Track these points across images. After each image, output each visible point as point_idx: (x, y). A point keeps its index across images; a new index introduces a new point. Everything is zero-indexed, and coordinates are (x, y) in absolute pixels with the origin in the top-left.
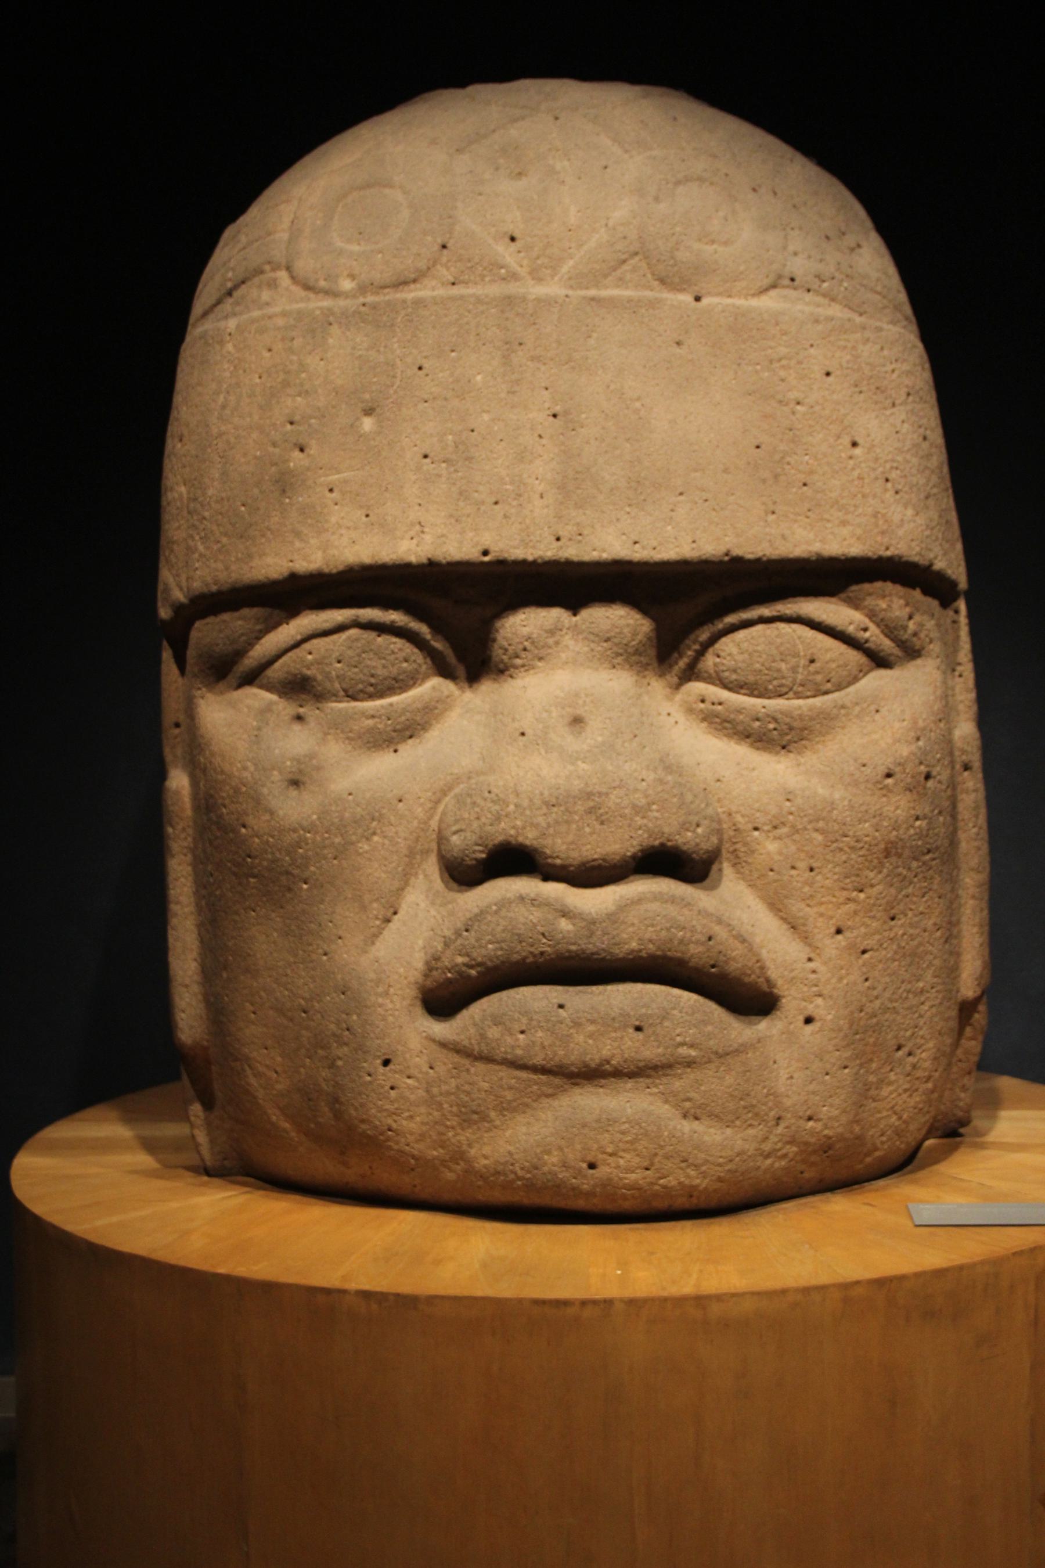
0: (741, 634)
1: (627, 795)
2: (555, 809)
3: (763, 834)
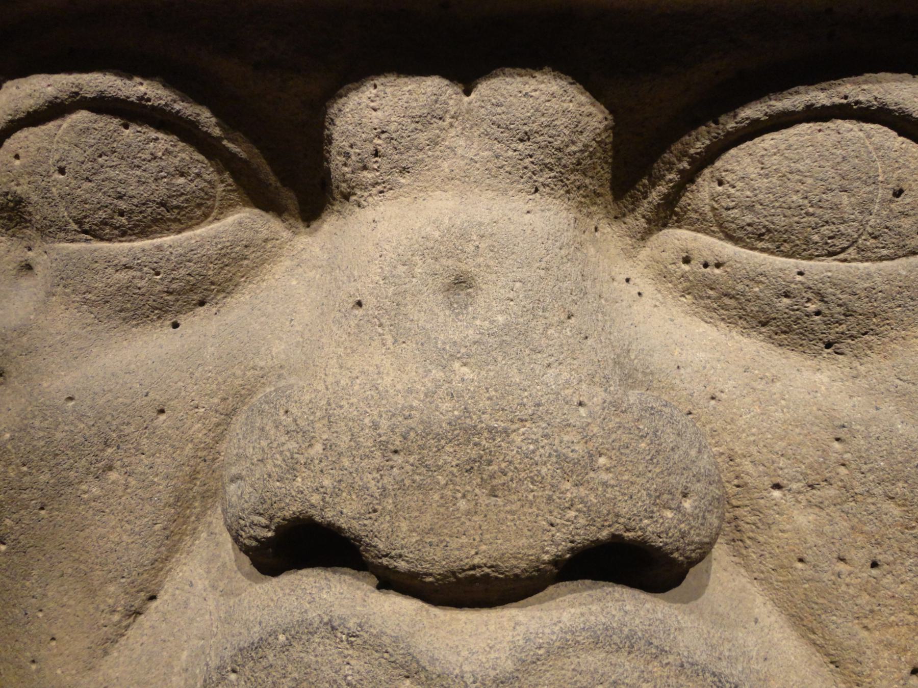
0: (768, 141)
1: (546, 436)
2: (398, 459)
3: (789, 496)
